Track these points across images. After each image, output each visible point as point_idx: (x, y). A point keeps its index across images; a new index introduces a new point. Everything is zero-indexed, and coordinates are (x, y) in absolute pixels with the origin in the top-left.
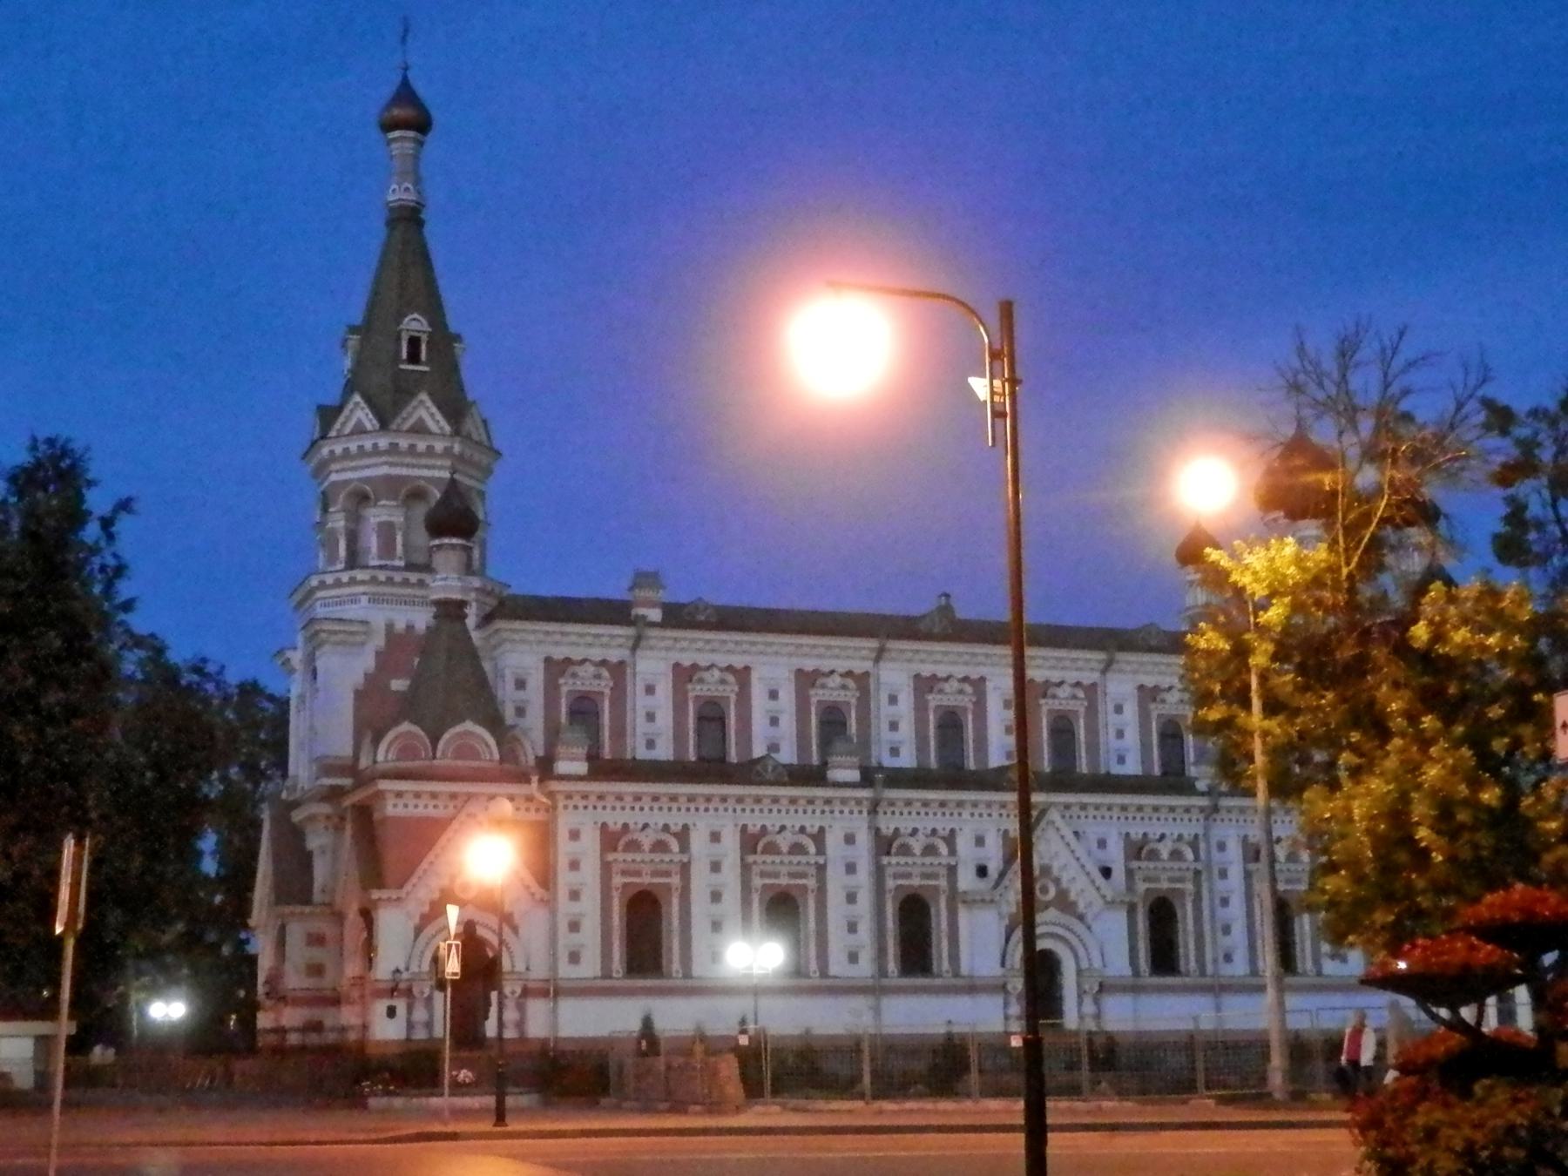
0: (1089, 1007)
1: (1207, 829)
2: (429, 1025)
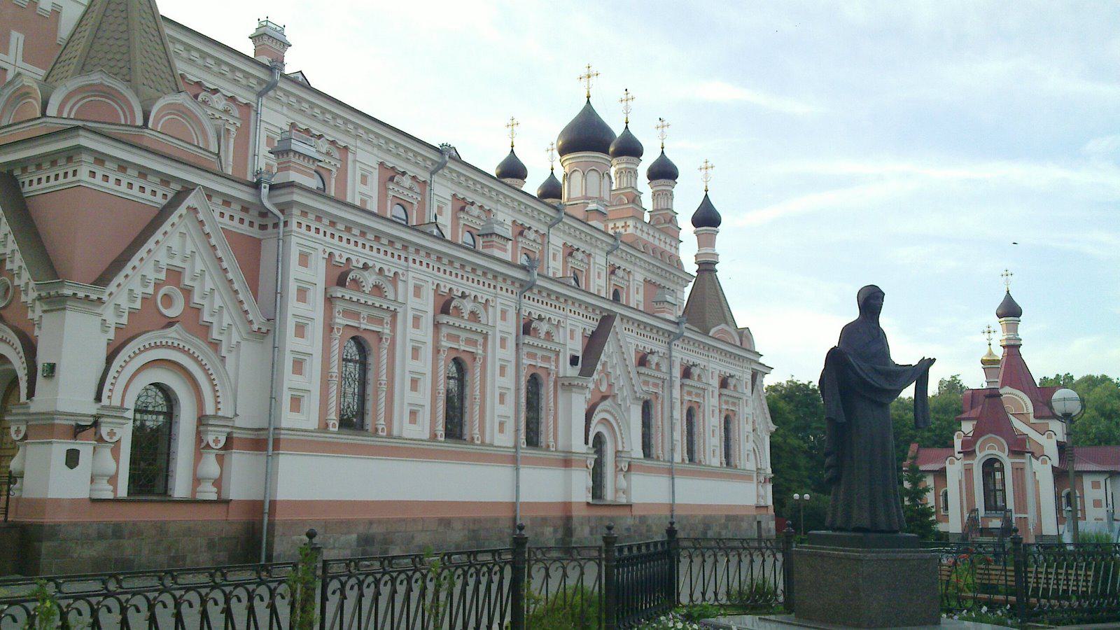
1: (670, 350)
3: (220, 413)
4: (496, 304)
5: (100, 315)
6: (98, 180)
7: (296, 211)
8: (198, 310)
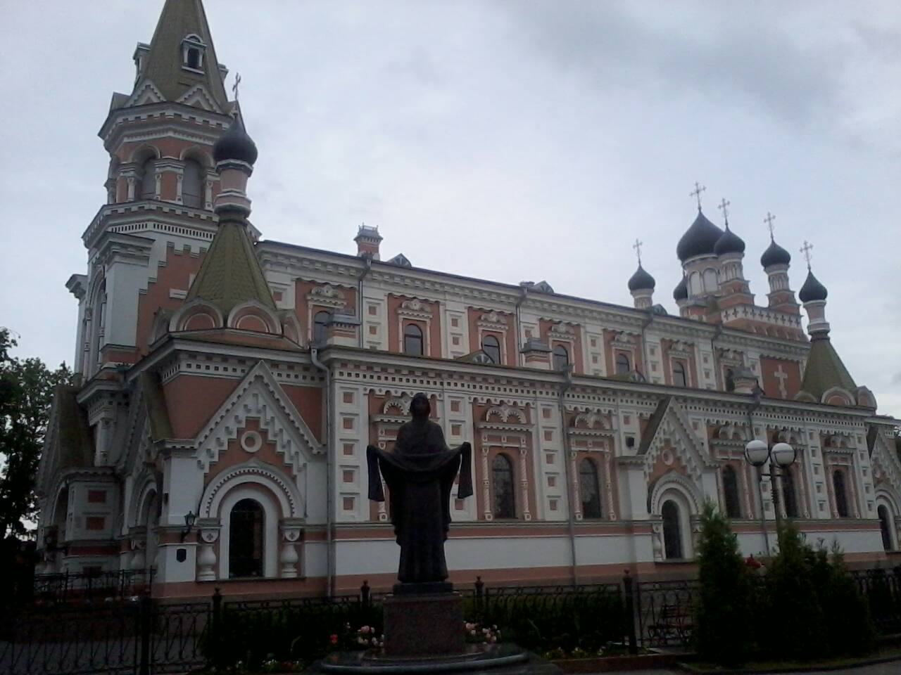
1: (750, 420)
2: (215, 567)
3: (295, 516)
4: (537, 405)
5: (196, 458)
6: (194, 369)
7: (337, 365)
8: (273, 445)
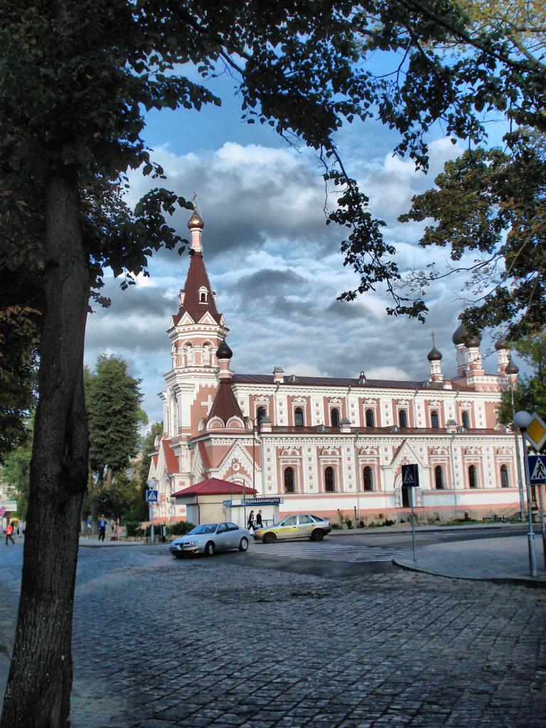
0: (419, 499)
8: (243, 468)
